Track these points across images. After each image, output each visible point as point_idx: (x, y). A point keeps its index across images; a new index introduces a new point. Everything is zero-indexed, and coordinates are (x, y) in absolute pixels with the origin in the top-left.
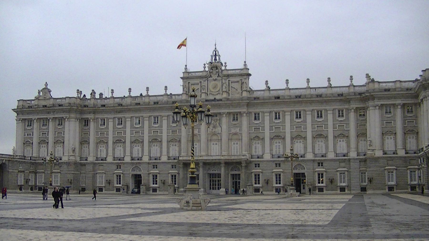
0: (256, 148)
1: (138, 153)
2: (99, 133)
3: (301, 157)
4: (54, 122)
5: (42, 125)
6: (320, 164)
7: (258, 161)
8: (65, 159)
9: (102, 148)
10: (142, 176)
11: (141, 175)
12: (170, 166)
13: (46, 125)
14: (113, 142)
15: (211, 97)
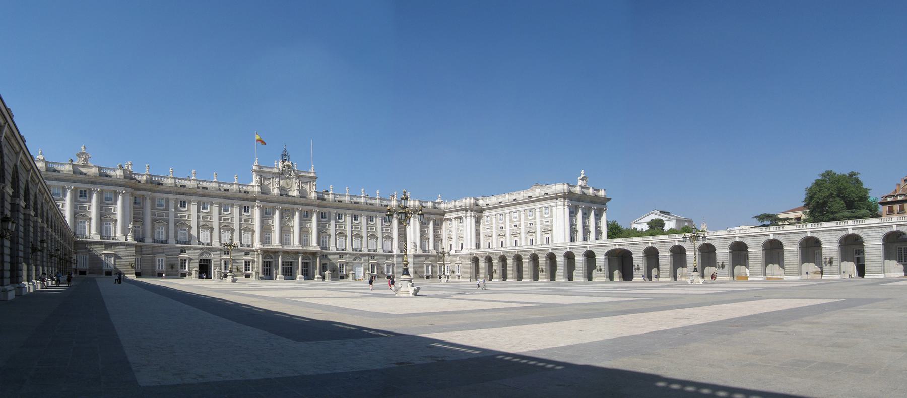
0: (323, 242)
1: (207, 239)
2: (156, 213)
3: (360, 251)
4: (100, 195)
5: (78, 196)
6: (373, 257)
7: (326, 253)
8: (123, 240)
9: (160, 230)
10: (213, 261)
11: (210, 260)
12: (244, 253)
13: (85, 197)
14: (175, 224)
15: (283, 193)
